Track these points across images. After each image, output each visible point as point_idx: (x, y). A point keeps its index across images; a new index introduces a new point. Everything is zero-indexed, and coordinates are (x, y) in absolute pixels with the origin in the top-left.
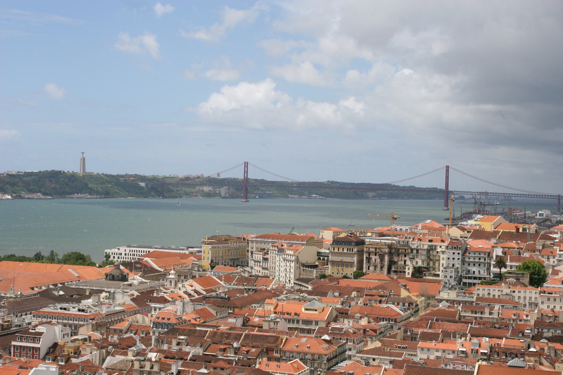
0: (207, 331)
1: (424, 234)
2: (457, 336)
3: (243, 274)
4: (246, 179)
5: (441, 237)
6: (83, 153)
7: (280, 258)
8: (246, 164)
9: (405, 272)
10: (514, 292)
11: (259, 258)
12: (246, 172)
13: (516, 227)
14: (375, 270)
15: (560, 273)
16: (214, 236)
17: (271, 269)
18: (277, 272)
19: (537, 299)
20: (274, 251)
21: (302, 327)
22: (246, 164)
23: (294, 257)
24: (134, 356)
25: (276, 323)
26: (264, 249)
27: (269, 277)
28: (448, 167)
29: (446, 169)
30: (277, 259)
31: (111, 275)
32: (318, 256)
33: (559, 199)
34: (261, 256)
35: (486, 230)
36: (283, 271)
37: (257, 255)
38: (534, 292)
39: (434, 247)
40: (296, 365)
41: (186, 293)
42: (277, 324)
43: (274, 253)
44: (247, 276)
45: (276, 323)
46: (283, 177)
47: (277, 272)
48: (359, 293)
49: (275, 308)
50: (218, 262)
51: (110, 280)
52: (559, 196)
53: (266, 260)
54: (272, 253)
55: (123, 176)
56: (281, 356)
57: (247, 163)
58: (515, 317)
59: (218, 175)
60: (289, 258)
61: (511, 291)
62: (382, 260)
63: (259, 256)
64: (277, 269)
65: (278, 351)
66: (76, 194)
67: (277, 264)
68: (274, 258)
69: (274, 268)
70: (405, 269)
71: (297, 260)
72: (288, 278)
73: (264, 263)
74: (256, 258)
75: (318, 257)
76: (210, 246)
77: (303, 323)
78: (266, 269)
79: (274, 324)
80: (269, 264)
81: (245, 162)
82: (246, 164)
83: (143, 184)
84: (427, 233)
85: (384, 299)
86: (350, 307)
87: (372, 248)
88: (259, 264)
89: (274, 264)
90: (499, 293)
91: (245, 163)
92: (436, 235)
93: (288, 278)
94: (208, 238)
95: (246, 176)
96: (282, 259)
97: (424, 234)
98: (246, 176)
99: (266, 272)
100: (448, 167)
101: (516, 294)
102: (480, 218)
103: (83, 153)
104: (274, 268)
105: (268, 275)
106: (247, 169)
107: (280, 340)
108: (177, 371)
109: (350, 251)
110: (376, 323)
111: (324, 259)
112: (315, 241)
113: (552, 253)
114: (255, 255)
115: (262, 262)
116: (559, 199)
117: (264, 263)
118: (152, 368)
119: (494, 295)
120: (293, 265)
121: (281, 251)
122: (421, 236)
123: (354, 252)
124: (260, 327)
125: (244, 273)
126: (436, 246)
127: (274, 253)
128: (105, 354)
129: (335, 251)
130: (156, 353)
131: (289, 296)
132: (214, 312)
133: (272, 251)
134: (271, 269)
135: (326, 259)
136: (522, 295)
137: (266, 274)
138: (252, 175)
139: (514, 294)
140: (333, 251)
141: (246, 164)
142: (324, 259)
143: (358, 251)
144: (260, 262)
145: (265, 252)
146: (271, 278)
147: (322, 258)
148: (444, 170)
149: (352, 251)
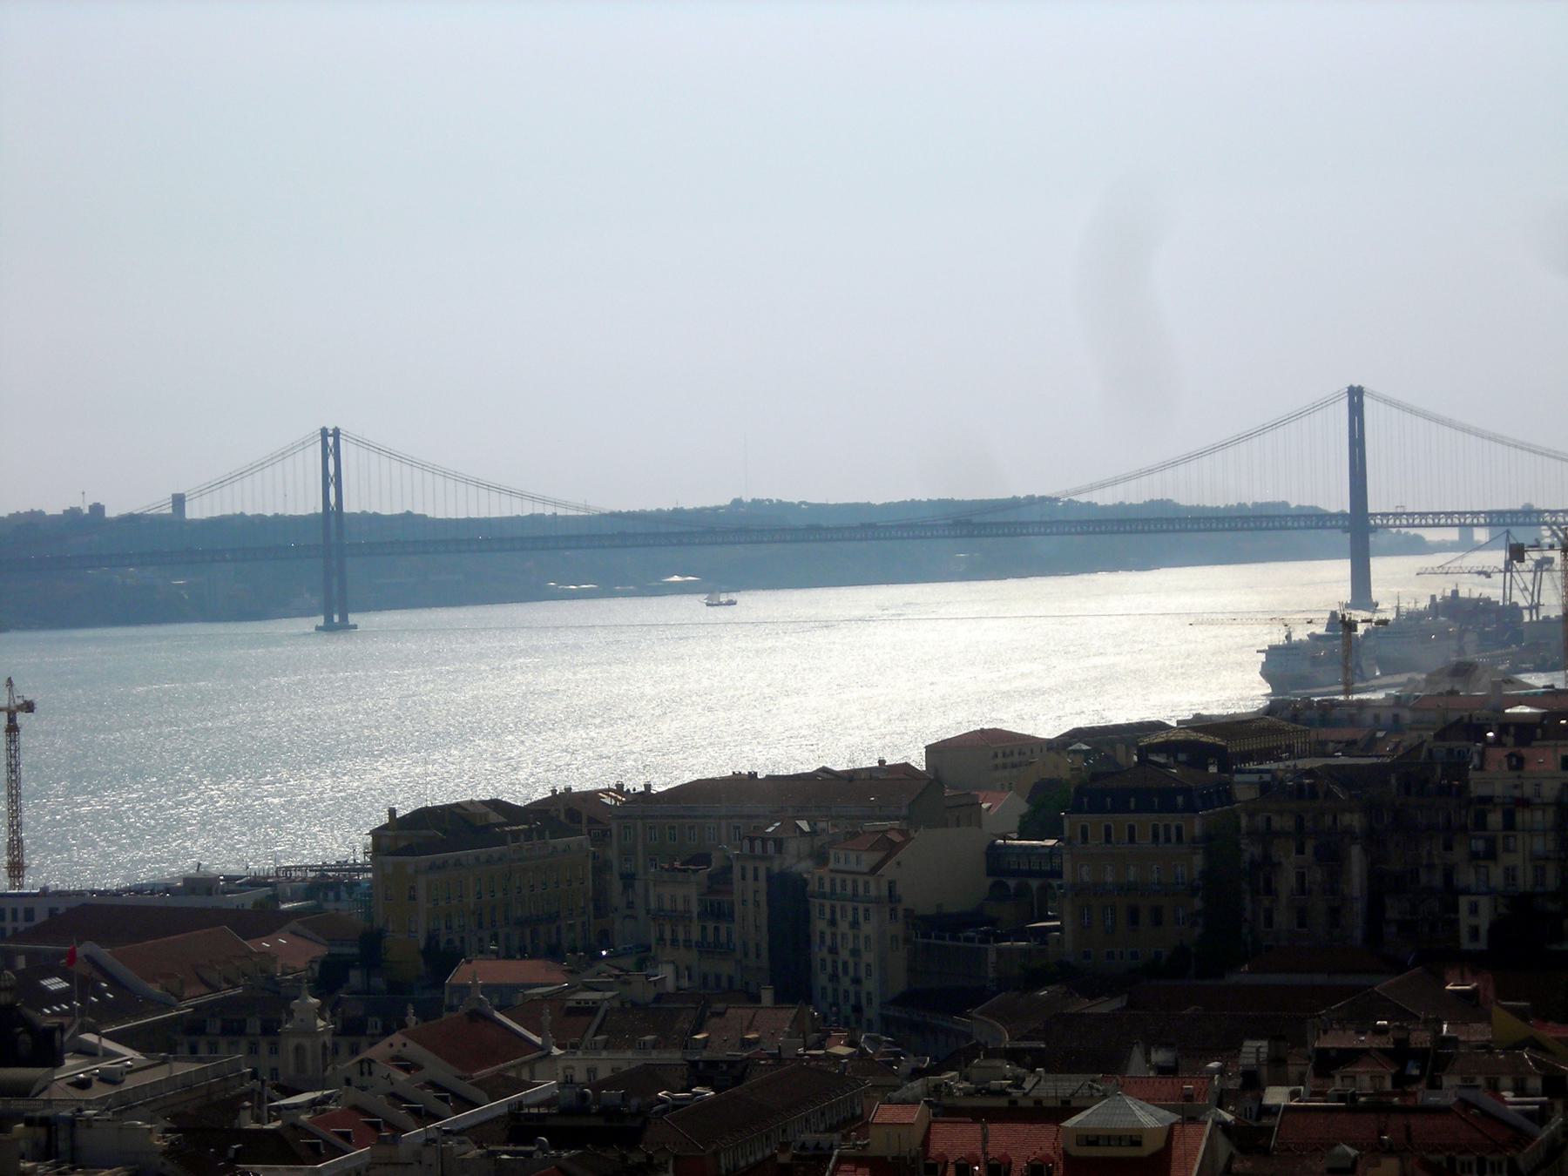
8: (331, 440)
12: (332, 480)
14: (1302, 924)
22: (331, 440)
28: (1356, 397)
32: (989, 874)
41: (396, 1098)
46: (522, 496)
50: (462, 940)
57: (336, 433)
59: (179, 501)
70: (1456, 910)
75: (990, 881)
82: (330, 442)
91: (324, 432)
100: (1356, 397)
117: (711, 925)
131: (952, 1079)
141: (330, 442)
148: (1343, 407)
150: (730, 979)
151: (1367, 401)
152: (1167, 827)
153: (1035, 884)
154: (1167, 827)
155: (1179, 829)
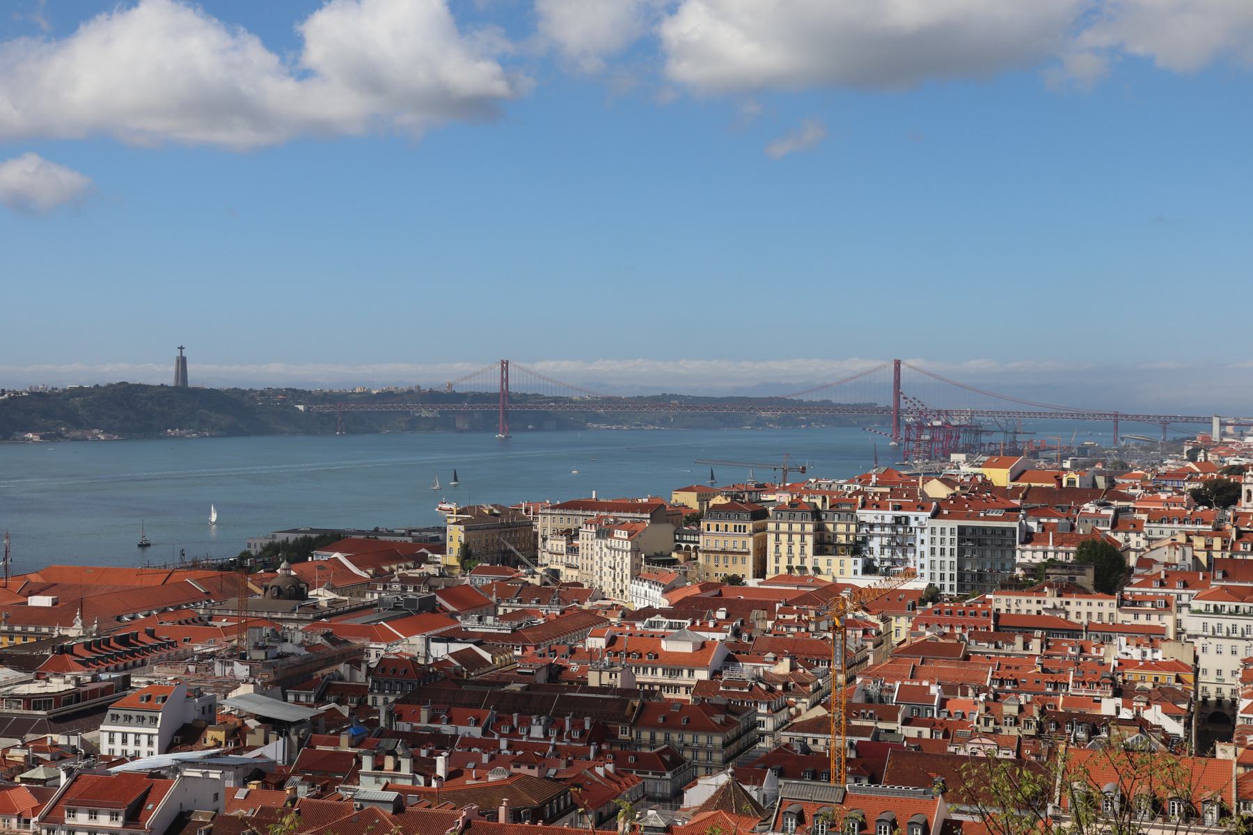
0: (484, 693)
1: (881, 493)
2: (970, 692)
3: (530, 580)
5: (916, 499)
6: (181, 348)
7: (601, 548)
8: (505, 365)
10: (1068, 603)
11: (560, 549)
12: (505, 380)
13: (1055, 477)
15: (1154, 566)
16: (470, 507)
17: (585, 569)
18: (597, 574)
19: (1113, 616)
20: (590, 534)
21: (664, 681)
22: (505, 365)
23: (629, 543)
24: (352, 747)
25: (613, 675)
26: (569, 531)
27: (582, 586)
29: (895, 366)
30: (597, 549)
31: (274, 588)
33: (1116, 421)
34: (564, 543)
35: (995, 485)
36: (608, 574)
37: (555, 543)
38: (1106, 603)
39: (903, 519)
40: (667, 758)
42: (616, 677)
43: (590, 538)
44: (538, 584)
45: (613, 675)
47: (597, 574)
48: (765, 612)
51: (273, 598)
53: (573, 550)
54: (585, 538)
55: (262, 393)
56: (632, 738)
58: (1074, 653)
61: (1062, 602)
63: (560, 543)
64: (596, 568)
65: (626, 728)
66: (169, 431)
67: (597, 558)
68: (589, 547)
69: (589, 568)
71: (635, 551)
72: (618, 587)
73: (570, 557)
74: (555, 549)
76: (462, 528)
77: (663, 674)
78: (577, 568)
79: (611, 677)
80: (580, 558)
81: (503, 362)
82: (505, 365)
83: (301, 407)
84: (887, 493)
86: (750, 638)
88: (559, 560)
89: (590, 558)
90: (1040, 607)
91: (503, 362)
92: (905, 496)
93: (618, 587)
94: (457, 511)
95: (505, 388)
96: (605, 550)
97: (883, 495)
98: (505, 388)
99: (575, 573)
101: (1073, 608)
102: (983, 462)
103: (181, 348)
104: (589, 568)
105: (579, 581)
106: (507, 374)
107: (629, 707)
108: (448, 774)
109: (740, 531)
110: (807, 671)
111: (688, 548)
112: (668, 514)
113: (1134, 526)
114: (552, 542)
115: (565, 557)
116: (1116, 421)
118: (397, 767)
119: (1028, 611)
120: (628, 560)
121: (604, 533)
122: (877, 499)
123: (747, 532)
124: (584, 683)
125: (533, 577)
126: (907, 518)
127: (590, 538)
128: (296, 744)
129: (711, 531)
130: (397, 740)
132: (487, 656)
133: (585, 534)
134: (585, 569)
135: (692, 546)
136: (1084, 609)
137: (574, 580)
138: (517, 384)
139: (1068, 608)
140: (706, 531)
141: (505, 365)
142: (688, 548)
143: (756, 530)
145: (571, 535)
146: (586, 587)
147: (684, 545)
149: (744, 531)
150: (577, 577)
151: (901, 365)
152: (740, 526)
153: (692, 546)
154: (740, 526)
155: (744, 527)
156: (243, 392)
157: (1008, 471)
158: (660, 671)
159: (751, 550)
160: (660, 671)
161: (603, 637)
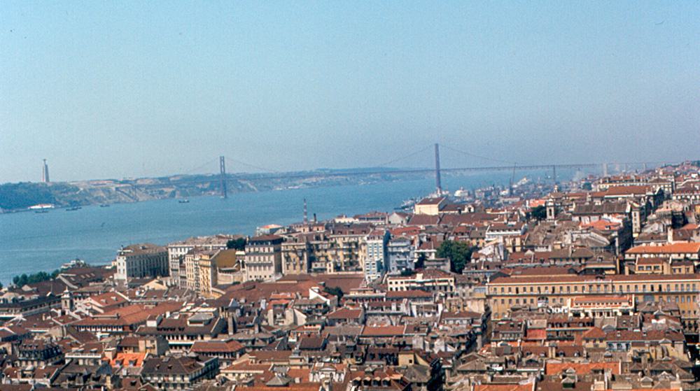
4: (223, 174)
6: (45, 160)
9: (326, 269)
12: (223, 166)
28: (437, 146)
33: (554, 169)
49: (159, 324)
52: (554, 167)
60: (205, 263)
62: (301, 258)
82: (222, 159)
85: (290, 302)
87: (290, 246)
91: (221, 157)
100: (437, 146)
103: (45, 160)
116: (554, 169)
120: (209, 271)
141: (222, 159)
143: (275, 251)
144: (177, 270)
148: (434, 147)
156: (16, 186)
157: (437, 205)
158: (185, 338)
159: (273, 263)
160: (185, 338)
161: (155, 320)
